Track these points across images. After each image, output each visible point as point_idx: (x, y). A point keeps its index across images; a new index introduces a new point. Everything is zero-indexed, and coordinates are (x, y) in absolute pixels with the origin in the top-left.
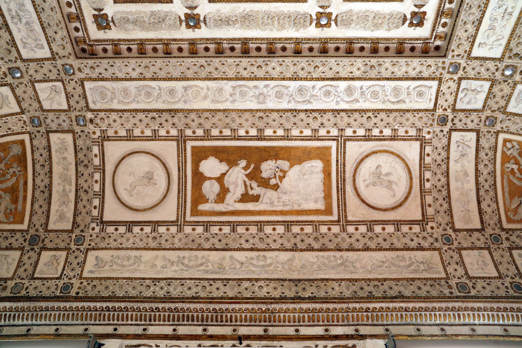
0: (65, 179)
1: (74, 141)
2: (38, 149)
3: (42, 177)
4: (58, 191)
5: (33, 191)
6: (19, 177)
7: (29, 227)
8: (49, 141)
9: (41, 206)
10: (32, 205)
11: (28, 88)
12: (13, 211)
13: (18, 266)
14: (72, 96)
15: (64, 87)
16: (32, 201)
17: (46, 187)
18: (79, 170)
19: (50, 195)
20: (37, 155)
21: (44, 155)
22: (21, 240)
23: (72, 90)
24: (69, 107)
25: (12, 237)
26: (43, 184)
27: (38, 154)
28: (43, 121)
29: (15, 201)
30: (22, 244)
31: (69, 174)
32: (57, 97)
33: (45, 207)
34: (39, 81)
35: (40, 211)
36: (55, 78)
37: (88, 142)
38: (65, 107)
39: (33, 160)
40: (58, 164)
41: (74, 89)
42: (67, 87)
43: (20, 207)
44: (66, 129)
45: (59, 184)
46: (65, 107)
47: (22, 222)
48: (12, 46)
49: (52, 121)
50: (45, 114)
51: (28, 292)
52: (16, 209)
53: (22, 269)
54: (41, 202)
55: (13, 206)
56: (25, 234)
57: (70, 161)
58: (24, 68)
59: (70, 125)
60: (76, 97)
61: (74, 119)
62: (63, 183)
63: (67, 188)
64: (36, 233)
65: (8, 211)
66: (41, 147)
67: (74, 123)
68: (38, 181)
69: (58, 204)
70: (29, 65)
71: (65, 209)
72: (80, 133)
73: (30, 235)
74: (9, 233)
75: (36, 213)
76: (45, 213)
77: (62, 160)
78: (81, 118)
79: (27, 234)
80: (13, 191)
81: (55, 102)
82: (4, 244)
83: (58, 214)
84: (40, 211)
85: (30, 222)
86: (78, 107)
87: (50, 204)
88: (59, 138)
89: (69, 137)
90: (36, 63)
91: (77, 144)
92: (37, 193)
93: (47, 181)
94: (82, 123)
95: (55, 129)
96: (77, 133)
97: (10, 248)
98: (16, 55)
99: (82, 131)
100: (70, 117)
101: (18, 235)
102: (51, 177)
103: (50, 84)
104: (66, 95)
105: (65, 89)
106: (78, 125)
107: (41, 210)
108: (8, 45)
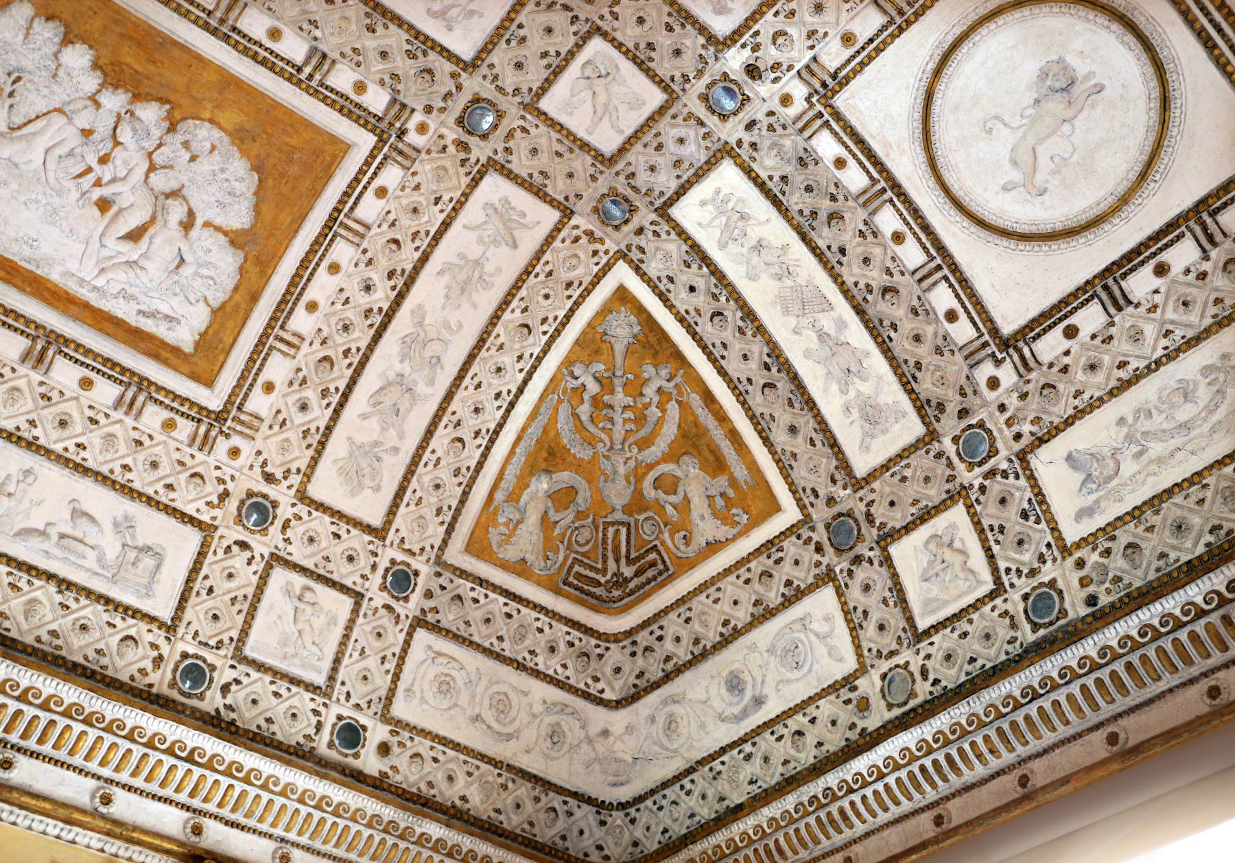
0: (804, 304)
1: (748, 172)
2: (671, 279)
3: (737, 347)
4: (807, 354)
5: (744, 403)
6: (680, 393)
7: (802, 507)
8: (682, 233)
9: (793, 430)
10: (766, 441)
11: (533, 131)
12: (731, 493)
13: (854, 630)
14: (651, 46)
15: (613, 41)
16: (760, 433)
17: (767, 367)
18: (822, 244)
19: (795, 378)
20: (682, 299)
21: (700, 283)
22: (809, 555)
23: (638, 30)
24: (666, 89)
25: (778, 561)
26: (753, 365)
27: (684, 294)
28: (629, 193)
29: (716, 465)
30: (818, 564)
31: (801, 281)
32: (615, 88)
33: (807, 424)
34: (543, 91)
35: (799, 444)
36: (572, 40)
37: (788, 143)
38: (656, 97)
39: (681, 320)
40: (753, 278)
41: (641, 21)
42: (619, 36)
43: (740, 472)
44: (703, 159)
45: (796, 332)
46: (656, 97)
47: (774, 507)
48: (425, 54)
49: (652, 169)
50: (620, 166)
51: (936, 682)
52: (733, 482)
53: (871, 629)
54: (784, 417)
55: (722, 482)
56: (806, 533)
57: (777, 242)
58: (487, 84)
59: (706, 136)
60: (665, 41)
61: (701, 111)
62: (805, 321)
63: (826, 322)
64: (836, 509)
65: (720, 502)
66: (675, 267)
67: (712, 121)
68: (734, 366)
69: (834, 387)
70: (491, 66)
71: (866, 388)
72: (747, 138)
73: (821, 527)
74: (763, 558)
75: (794, 455)
76: (818, 438)
77: (755, 259)
78: (718, 92)
79: (813, 529)
80: (692, 441)
81: (622, 108)
82: (772, 595)
83: (856, 414)
84: (799, 444)
85: (794, 492)
86: (688, 63)
87: (810, 404)
88: (703, 204)
89: (727, 176)
90: (503, 44)
91: (764, 175)
92: (757, 401)
93: (757, 348)
94: (729, 104)
95: (674, 185)
96: (739, 143)
97: (795, 595)
98: (449, 67)
99: (750, 126)
100: (690, 115)
101: (791, 547)
102: (761, 330)
103: (574, 69)
104: (634, 59)
105: (619, 46)
106: (724, 117)
107: (800, 439)
108: (415, 57)
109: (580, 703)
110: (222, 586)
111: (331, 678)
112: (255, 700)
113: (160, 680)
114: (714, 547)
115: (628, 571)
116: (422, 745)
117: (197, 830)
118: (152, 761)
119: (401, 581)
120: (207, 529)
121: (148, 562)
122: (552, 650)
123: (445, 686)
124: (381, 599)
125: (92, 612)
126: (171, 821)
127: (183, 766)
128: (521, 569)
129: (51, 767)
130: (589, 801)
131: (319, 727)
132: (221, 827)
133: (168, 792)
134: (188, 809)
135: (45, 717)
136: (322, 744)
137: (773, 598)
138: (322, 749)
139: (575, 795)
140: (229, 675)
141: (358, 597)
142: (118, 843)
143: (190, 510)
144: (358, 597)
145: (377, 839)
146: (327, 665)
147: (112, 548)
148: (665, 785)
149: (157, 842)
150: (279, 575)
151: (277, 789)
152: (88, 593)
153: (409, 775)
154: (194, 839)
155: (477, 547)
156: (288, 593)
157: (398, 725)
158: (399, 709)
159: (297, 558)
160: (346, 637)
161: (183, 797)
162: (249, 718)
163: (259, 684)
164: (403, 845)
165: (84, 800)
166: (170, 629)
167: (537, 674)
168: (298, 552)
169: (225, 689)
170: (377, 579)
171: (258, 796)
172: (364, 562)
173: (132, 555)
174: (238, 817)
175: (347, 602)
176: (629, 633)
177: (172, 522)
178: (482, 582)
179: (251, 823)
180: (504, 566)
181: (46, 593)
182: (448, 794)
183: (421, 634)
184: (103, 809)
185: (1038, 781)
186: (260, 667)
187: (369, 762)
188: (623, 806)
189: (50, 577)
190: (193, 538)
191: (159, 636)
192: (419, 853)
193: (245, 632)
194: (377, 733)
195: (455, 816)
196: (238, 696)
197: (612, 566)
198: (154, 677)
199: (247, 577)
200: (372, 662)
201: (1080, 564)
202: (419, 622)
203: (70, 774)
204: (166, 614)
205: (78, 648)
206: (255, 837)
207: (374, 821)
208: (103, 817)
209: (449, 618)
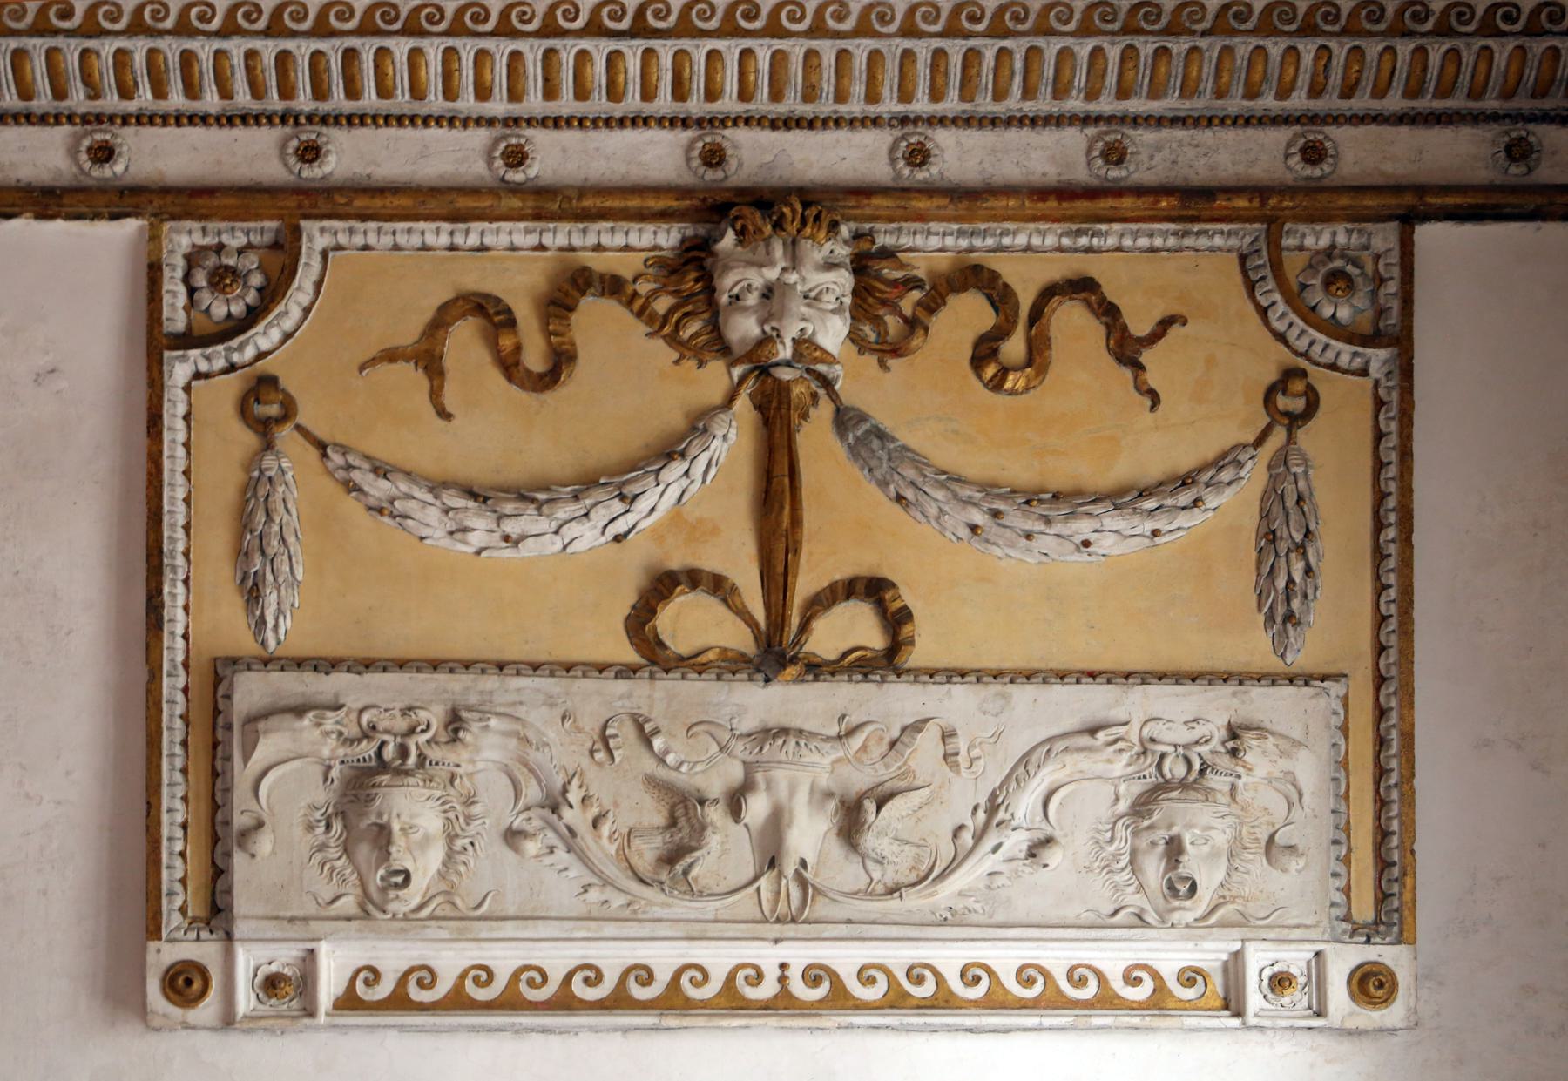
117: (714, 157)
118: (567, 59)
126: (659, 155)
127: (633, 51)
129: (393, 131)
132: (766, 136)
133: (632, 102)
134: (685, 123)
135: (333, 49)
142: (565, 227)
145: (1113, 54)
149: (634, 203)
151: (848, 25)
154: (711, 175)
161: (665, 103)
164: (1179, 46)
171: (811, 55)
174: (792, 104)
179: (825, 107)
184: (516, 176)
192: (1227, 51)
203: (433, 132)
206: (843, 134)
208: (516, 189)
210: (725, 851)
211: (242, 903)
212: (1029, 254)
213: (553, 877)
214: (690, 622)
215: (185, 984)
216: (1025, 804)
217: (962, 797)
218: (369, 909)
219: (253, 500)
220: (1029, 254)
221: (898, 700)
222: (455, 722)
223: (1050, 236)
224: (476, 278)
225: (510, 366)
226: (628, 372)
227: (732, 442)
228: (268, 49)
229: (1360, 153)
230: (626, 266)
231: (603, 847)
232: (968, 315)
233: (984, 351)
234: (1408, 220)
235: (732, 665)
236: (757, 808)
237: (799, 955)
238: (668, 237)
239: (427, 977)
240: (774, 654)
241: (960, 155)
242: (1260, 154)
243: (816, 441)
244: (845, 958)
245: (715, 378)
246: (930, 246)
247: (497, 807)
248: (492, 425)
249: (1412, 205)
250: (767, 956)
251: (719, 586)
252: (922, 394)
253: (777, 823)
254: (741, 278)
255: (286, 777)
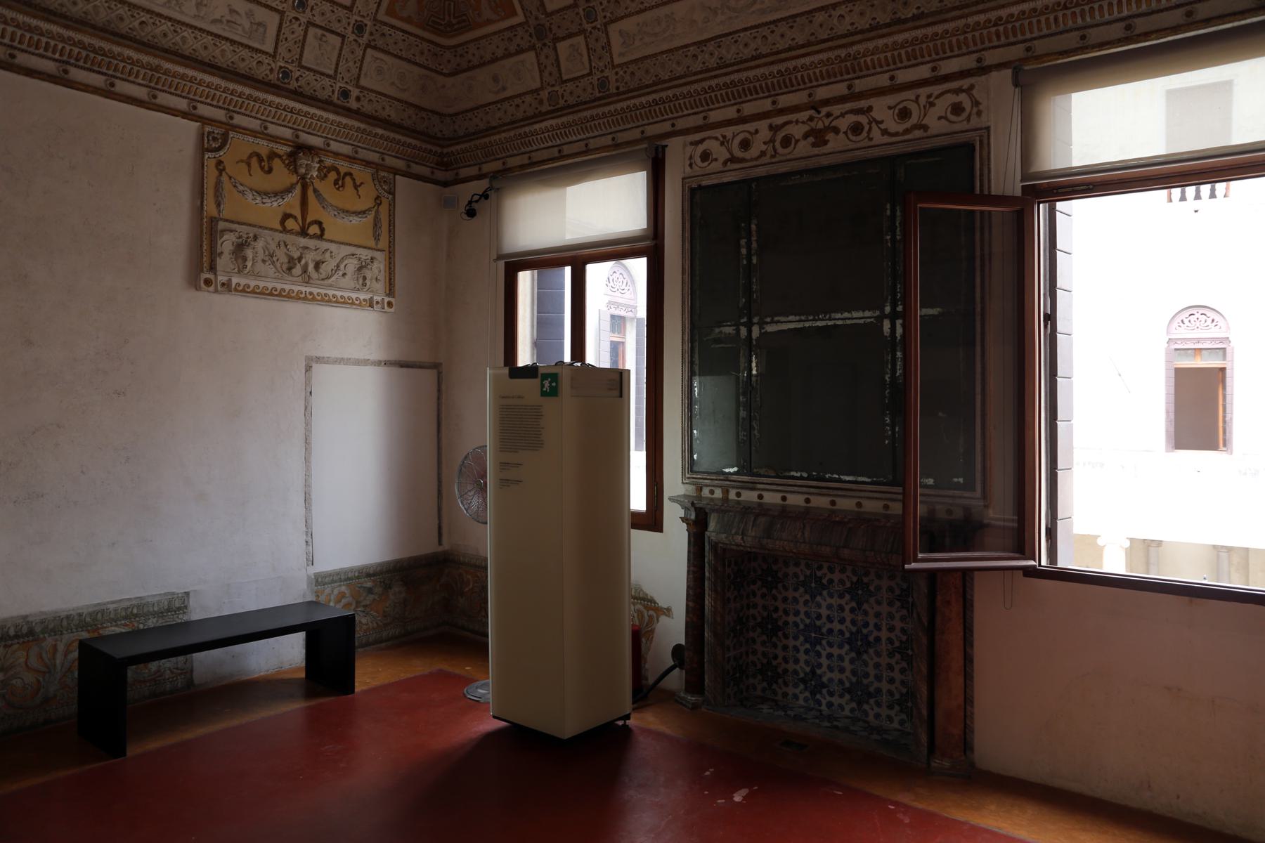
109: (433, 75)
110: (291, 37)
111: (336, 71)
112: (309, 82)
113: (273, 77)
114: (489, 22)
115: (454, 21)
116: (372, 96)
117: (297, 136)
119: (360, 28)
120: (282, 13)
121: (261, 30)
122: (422, 53)
123: (380, 71)
124: (352, 37)
125: (245, 53)
128: (408, 20)
130: (437, 113)
131: (333, 92)
136: (335, 98)
137: (512, 49)
138: (335, 100)
139: (432, 112)
140: (298, 74)
141: (343, 37)
143: (274, 5)
144: (343, 37)
146: (333, 67)
147: (247, 26)
148: (467, 111)
150: (312, 31)
152: (242, 45)
153: (368, 108)
155: (390, 12)
156: (315, 37)
157: (363, 88)
158: (363, 82)
159: (318, 22)
160: (340, 54)
162: (307, 90)
163: (309, 76)
165: (258, 128)
166: (274, 56)
167: (416, 64)
168: (318, 20)
169: (297, 80)
170: (350, 29)
172: (344, 21)
173: (255, 27)
175: (339, 40)
176: (454, 47)
177: (267, 11)
178: (393, 27)
180: (402, 19)
181: (226, 46)
182: (384, 114)
183: (369, 50)
185: (591, 146)
186: (309, 69)
187: (353, 104)
188: (450, 115)
189: (227, 39)
190: (276, 17)
191: (269, 60)
193: (301, 56)
194: (355, 93)
195: (386, 123)
196: (302, 82)
197: (447, 18)
198: (271, 77)
199: (300, 31)
200: (351, 64)
201: (617, 73)
202: (368, 46)
204: (271, 51)
205: (242, 67)
207: (358, 129)
209: (380, 43)
210: (297, 270)
211: (219, 268)
212: (344, 166)
213: (270, 270)
214: (290, 224)
215: (208, 282)
216: (342, 266)
217: (333, 263)
218: (239, 272)
219: (218, 186)
220: (344, 166)
221: (324, 245)
222: (255, 238)
223: (346, 164)
224: (257, 149)
225: (262, 168)
226: (282, 176)
227: (298, 191)
228: (230, 97)
229: (390, 161)
230: (281, 153)
231: (278, 265)
232: (333, 176)
233: (336, 183)
234: (395, 174)
235: (298, 234)
236: (303, 262)
237: (308, 289)
238: (289, 150)
239: (249, 287)
240: (303, 233)
241: (334, 146)
242: (374, 157)
243: (310, 193)
244: (315, 291)
245: (294, 178)
246: (329, 161)
247: (261, 255)
248: (258, 179)
249: (396, 172)
250: (303, 289)
251: (295, 218)
252: (326, 188)
253: (306, 265)
254: (303, 161)
255: (227, 244)
